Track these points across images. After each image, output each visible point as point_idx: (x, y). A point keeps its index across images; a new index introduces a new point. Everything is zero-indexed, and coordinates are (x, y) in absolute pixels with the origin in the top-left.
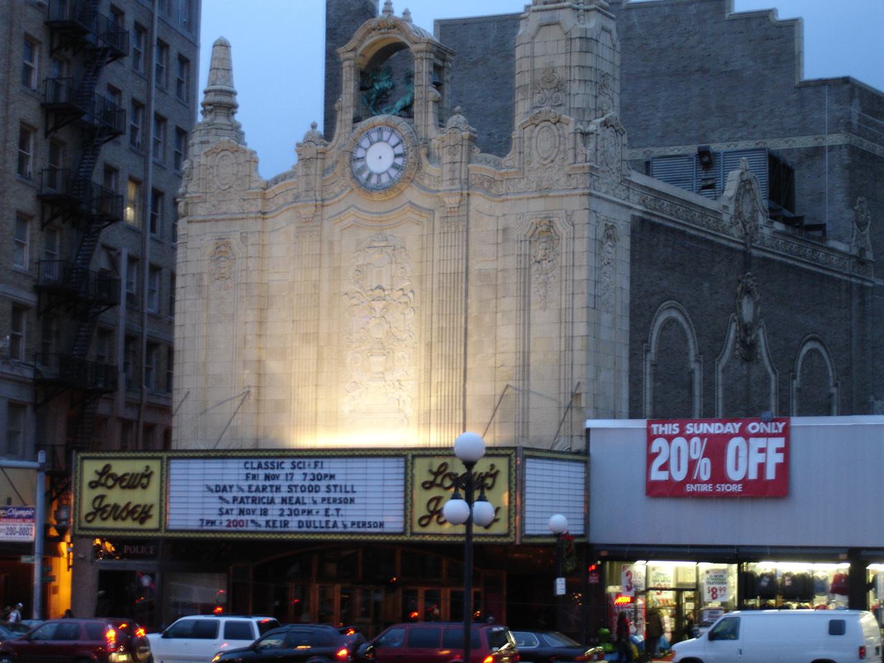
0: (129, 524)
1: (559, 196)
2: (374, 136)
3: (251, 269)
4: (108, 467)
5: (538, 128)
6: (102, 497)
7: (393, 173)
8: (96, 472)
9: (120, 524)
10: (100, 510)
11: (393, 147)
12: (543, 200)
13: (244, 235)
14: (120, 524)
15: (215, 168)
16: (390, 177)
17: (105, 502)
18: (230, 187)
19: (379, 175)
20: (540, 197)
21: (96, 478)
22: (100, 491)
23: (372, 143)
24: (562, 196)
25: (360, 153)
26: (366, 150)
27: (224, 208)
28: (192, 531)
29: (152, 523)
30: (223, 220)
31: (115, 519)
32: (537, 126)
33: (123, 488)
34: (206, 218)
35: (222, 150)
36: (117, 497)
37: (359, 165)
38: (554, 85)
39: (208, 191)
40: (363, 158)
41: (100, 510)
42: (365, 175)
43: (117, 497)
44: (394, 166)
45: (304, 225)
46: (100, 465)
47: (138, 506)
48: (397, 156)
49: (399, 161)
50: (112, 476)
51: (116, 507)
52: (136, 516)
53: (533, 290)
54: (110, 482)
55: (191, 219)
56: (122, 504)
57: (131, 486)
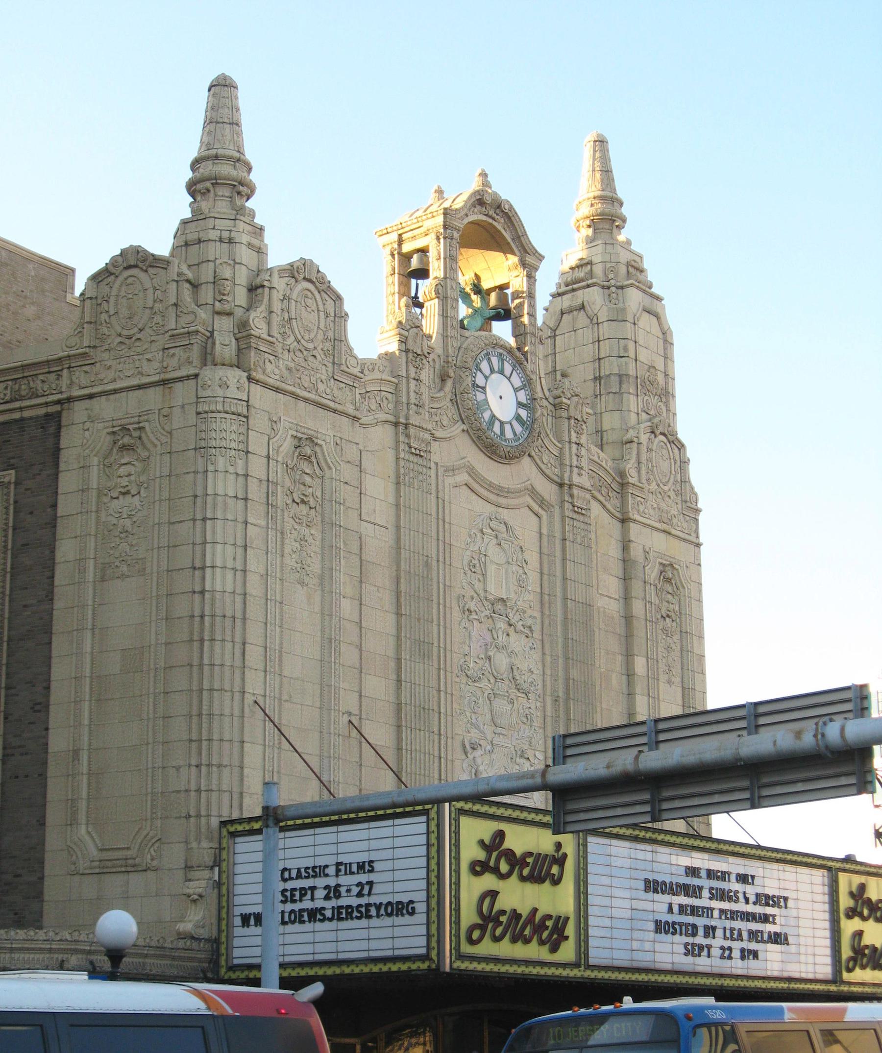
0: (533, 951)
4: (500, 835)
6: (493, 894)
8: (482, 843)
9: (520, 951)
10: (491, 920)
14: (520, 951)
17: (499, 905)
21: (481, 855)
22: (488, 881)
28: (619, 969)
29: (567, 952)
31: (514, 940)
33: (523, 879)
36: (516, 896)
41: (491, 920)
43: (516, 896)
45: (412, 458)
46: (485, 829)
47: (549, 917)
50: (509, 854)
51: (515, 915)
52: (545, 935)
54: (504, 867)
56: (525, 912)
57: (536, 878)
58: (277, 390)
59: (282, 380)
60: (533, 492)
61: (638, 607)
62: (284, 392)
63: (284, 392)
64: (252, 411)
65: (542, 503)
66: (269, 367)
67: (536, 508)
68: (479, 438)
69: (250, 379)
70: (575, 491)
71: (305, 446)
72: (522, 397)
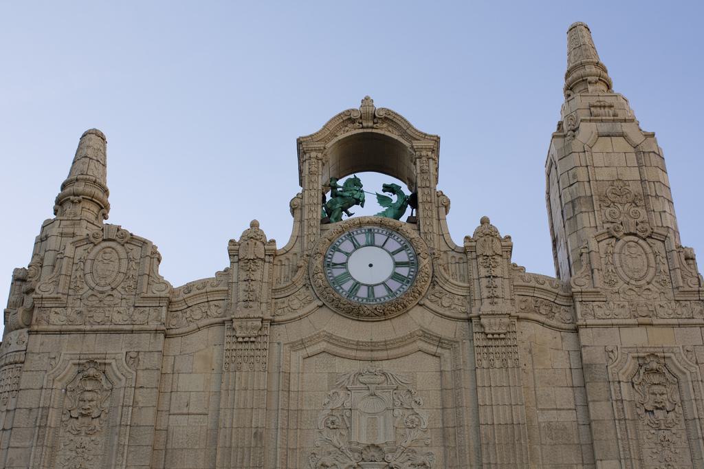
1: (667, 325)
2: (361, 239)
3: (140, 405)
5: (620, 243)
7: (394, 285)
11: (393, 254)
12: (642, 330)
13: (133, 355)
15: (89, 263)
16: (389, 290)
18: (113, 289)
19: (371, 288)
20: (639, 325)
23: (357, 247)
24: (673, 326)
25: (338, 258)
26: (348, 255)
27: (99, 316)
30: (96, 332)
32: (618, 239)
34: (64, 328)
35: (104, 240)
37: (337, 272)
38: (630, 200)
39: (71, 292)
40: (344, 265)
42: (347, 286)
44: (395, 276)
45: (240, 346)
48: (397, 264)
49: (404, 271)
53: (646, 453)
55: (36, 328)
58: (61, 332)
59: (72, 322)
60: (426, 335)
61: (600, 410)
62: (69, 332)
63: (69, 332)
64: (29, 356)
65: (440, 342)
66: (53, 318)
67: (433, 349)
68: (337, 307)
69: (30, 333)
70: (484, 321)
71: (91, 370)
72: (403, 257)
